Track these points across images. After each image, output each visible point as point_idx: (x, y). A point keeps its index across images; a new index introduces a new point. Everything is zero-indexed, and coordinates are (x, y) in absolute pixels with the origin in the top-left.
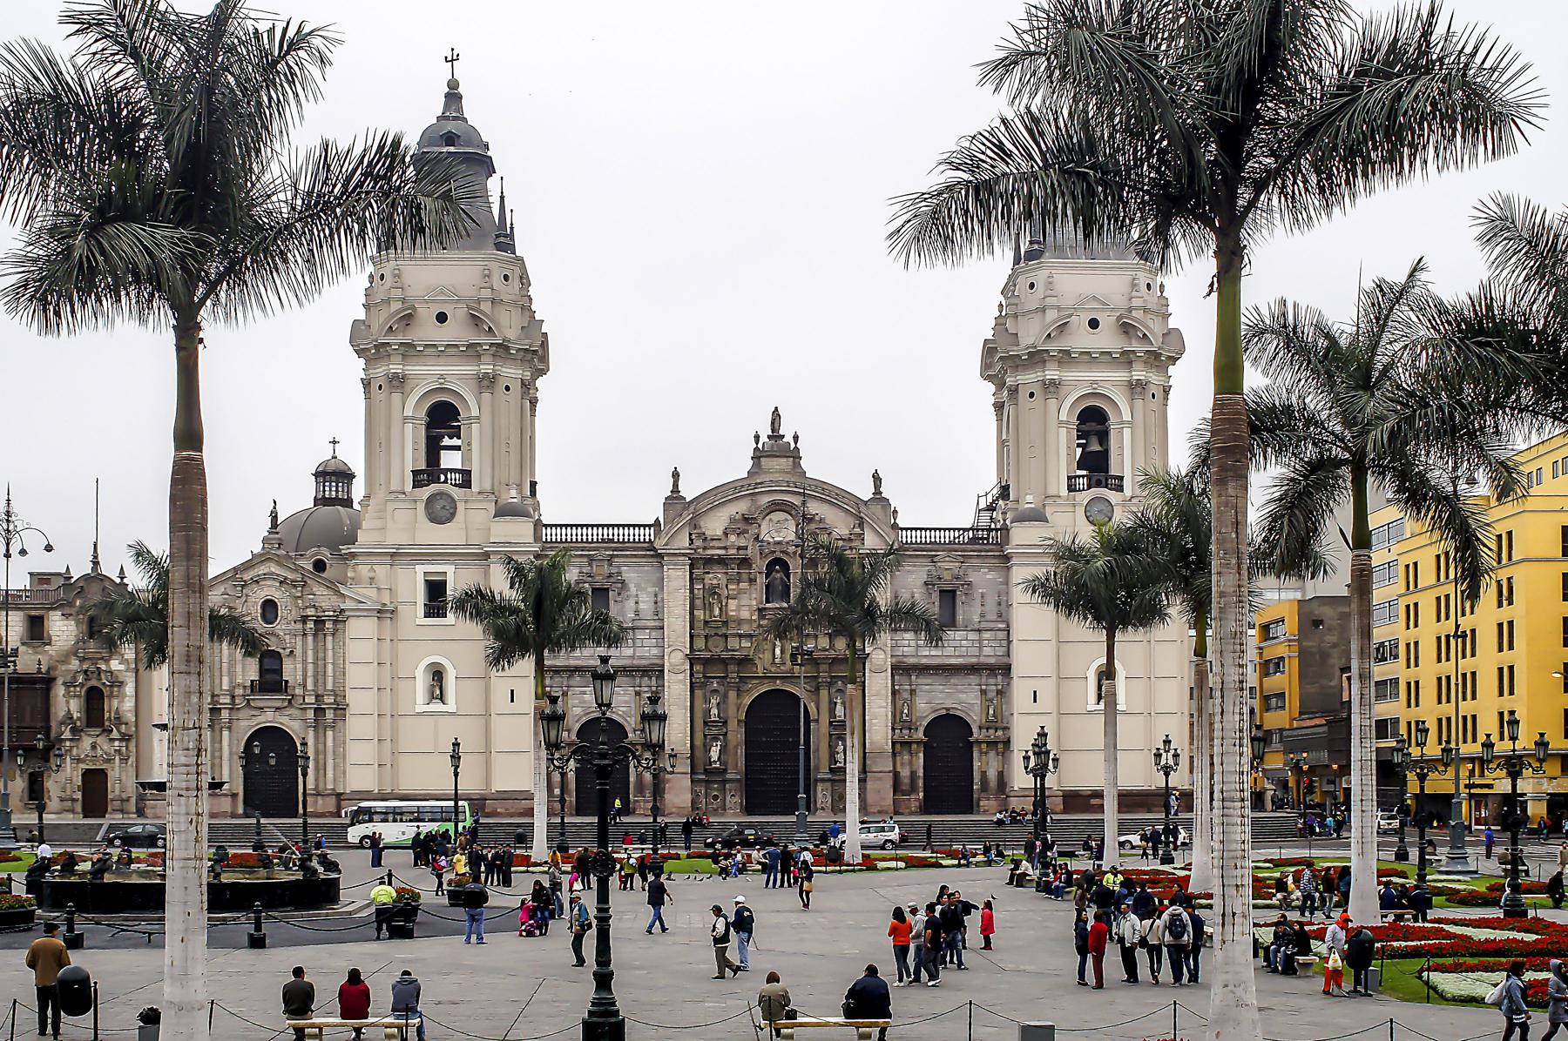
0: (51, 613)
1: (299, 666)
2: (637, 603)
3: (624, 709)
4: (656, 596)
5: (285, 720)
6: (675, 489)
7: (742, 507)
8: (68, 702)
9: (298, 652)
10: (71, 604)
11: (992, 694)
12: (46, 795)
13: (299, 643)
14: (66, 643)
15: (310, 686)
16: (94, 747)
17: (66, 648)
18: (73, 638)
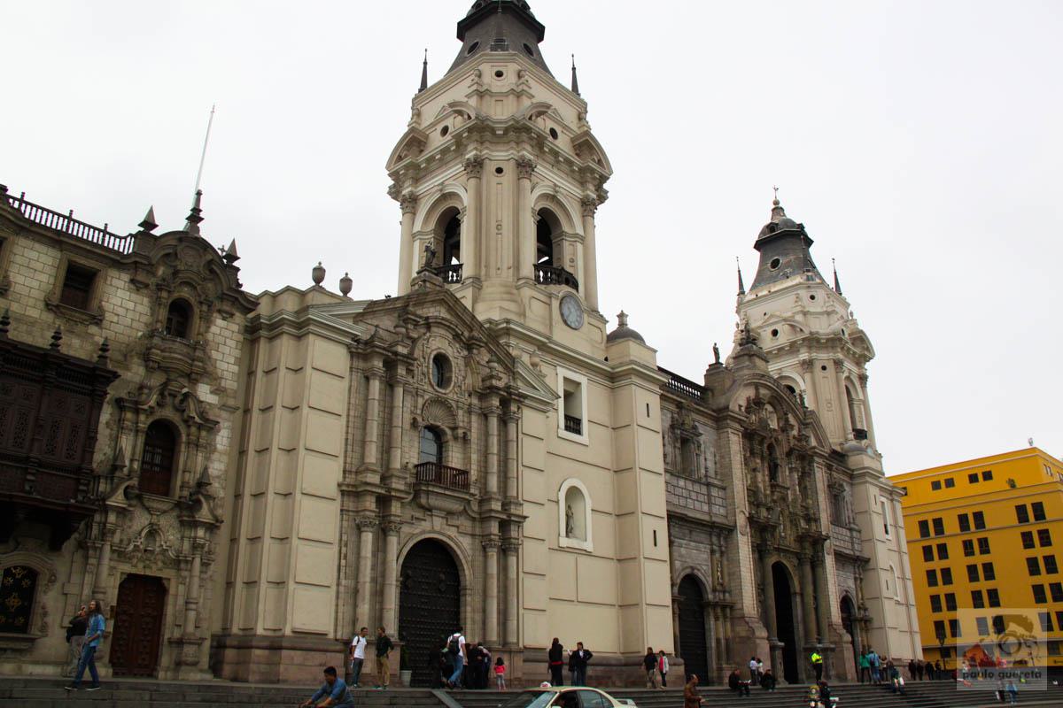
0: (113, 273)
1: (474, 457)
2: (706, 459)
3: (705, 568)
4: (715, 456)
5: (452, 532)
6: (718, 363)
7: (751, 392)
8: (116, 439)
9: (474, 436)
10: (150, 268)
11: (859, 582)
12: (37, 621)
13: (475, 425)
14: (128, 331)
15: (493, 483)
16: (153, 532)
17: (126, 340)
18: (141, 326)
